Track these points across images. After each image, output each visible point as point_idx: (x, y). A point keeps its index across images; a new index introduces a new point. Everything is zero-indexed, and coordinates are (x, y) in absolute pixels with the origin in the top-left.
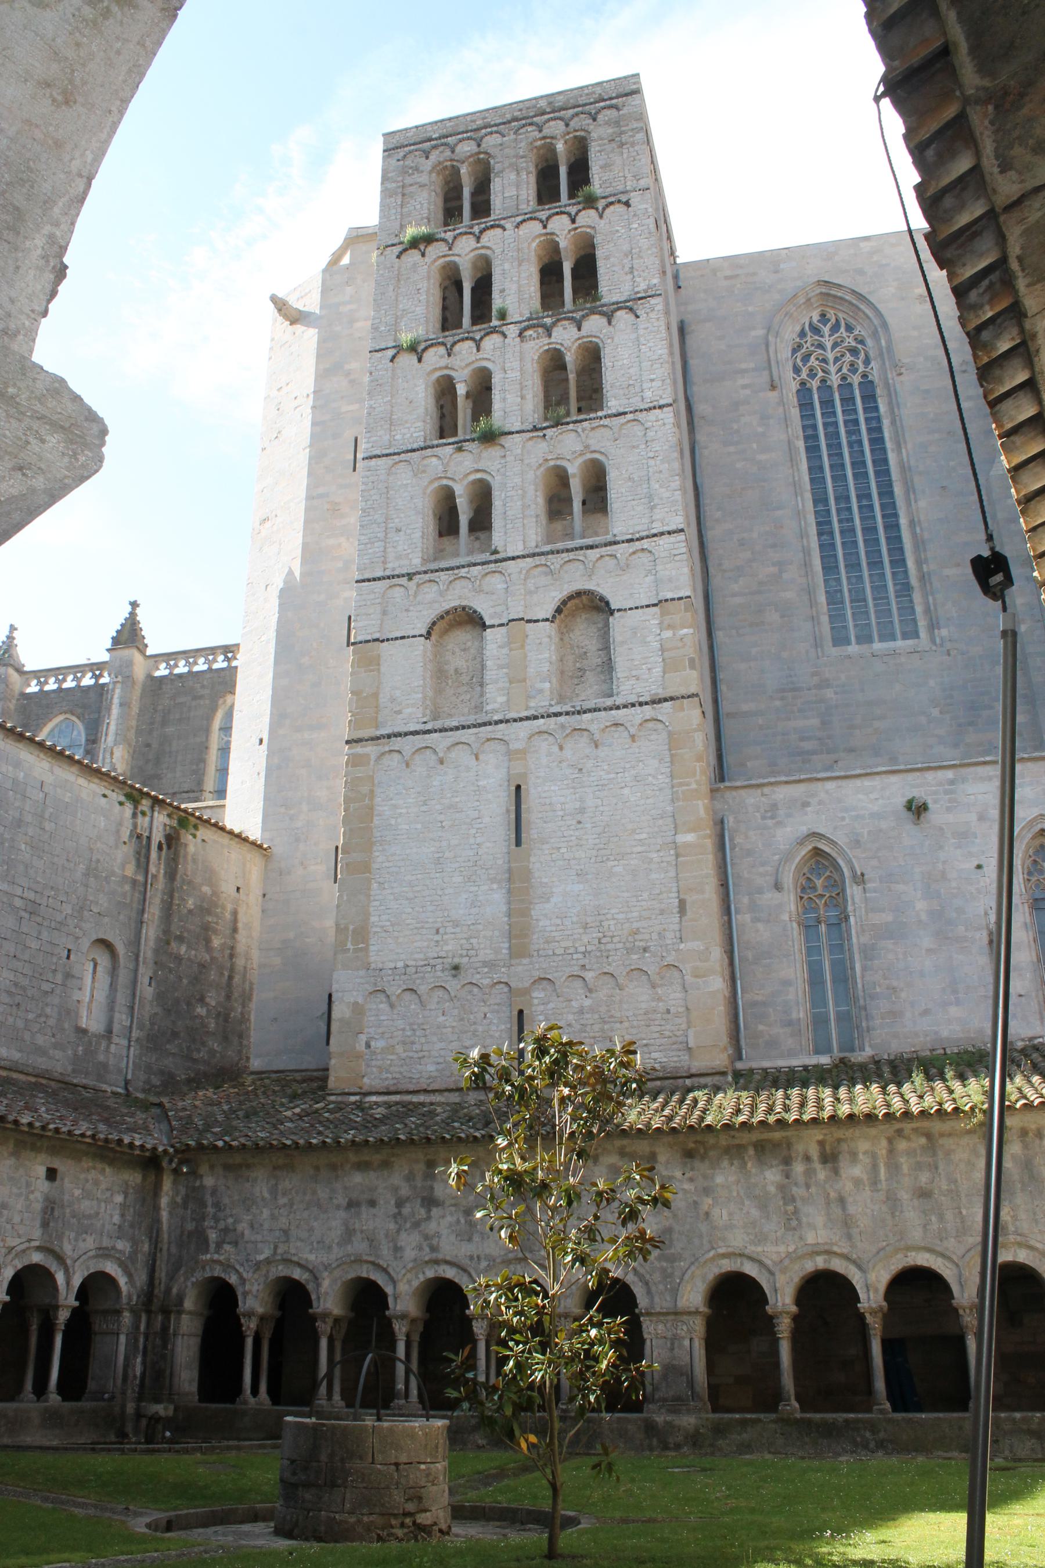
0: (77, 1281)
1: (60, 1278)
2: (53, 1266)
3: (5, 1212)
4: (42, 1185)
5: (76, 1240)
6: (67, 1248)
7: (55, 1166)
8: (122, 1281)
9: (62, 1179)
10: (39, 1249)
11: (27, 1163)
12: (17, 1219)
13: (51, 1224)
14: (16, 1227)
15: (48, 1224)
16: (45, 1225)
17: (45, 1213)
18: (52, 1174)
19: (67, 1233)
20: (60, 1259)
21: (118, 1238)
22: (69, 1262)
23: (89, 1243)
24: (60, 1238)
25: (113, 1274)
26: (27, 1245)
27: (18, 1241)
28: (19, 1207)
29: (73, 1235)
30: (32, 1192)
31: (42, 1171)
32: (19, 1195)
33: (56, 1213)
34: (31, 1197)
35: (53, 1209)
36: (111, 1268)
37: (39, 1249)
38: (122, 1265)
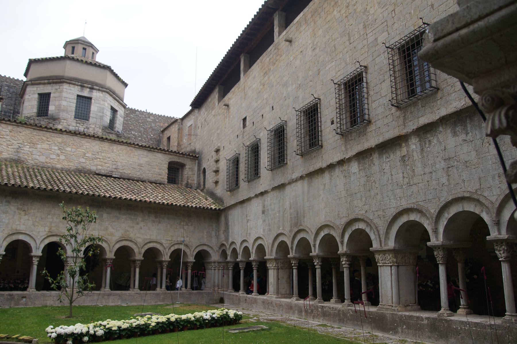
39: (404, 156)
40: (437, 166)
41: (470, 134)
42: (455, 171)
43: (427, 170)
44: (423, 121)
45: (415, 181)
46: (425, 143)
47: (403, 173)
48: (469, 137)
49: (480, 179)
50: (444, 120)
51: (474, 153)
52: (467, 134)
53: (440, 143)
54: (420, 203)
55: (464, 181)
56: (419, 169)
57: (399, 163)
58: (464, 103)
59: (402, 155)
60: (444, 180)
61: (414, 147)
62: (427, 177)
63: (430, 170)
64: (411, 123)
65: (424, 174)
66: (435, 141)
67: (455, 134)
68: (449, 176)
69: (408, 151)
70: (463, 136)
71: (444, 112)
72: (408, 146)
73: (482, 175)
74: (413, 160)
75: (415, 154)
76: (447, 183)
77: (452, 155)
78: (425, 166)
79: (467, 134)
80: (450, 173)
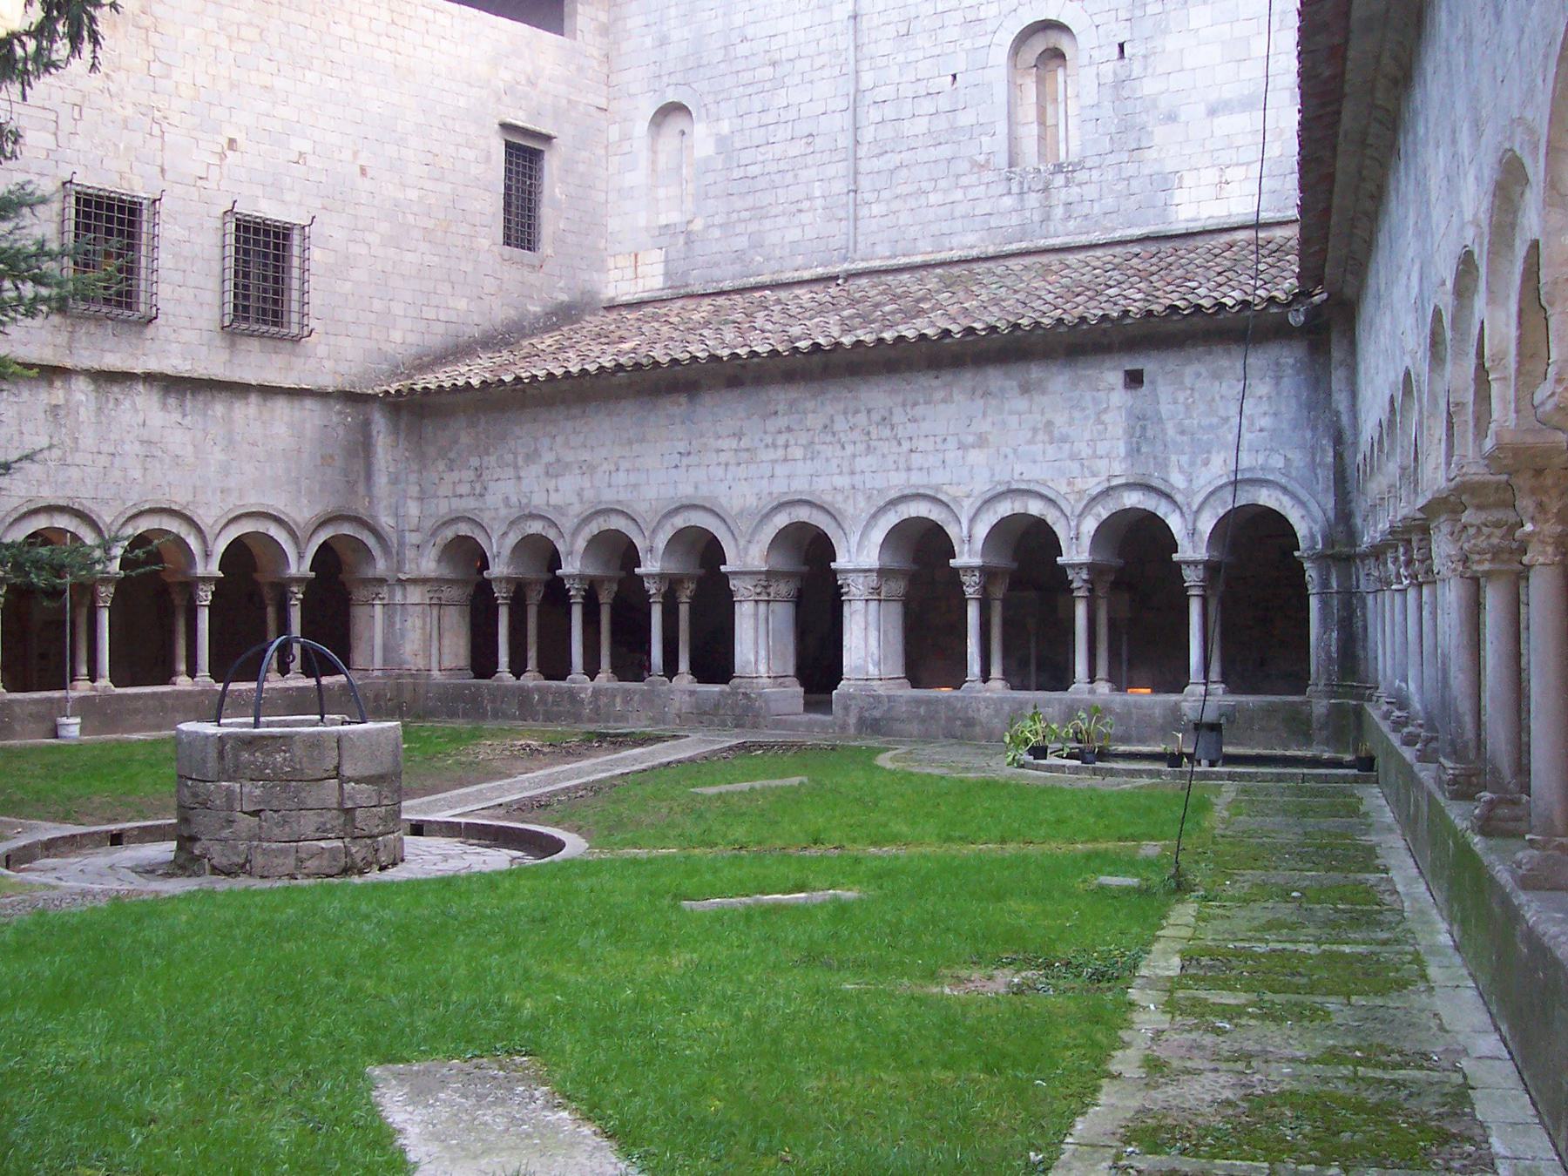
0: (1207, 524)
1: (1175, 523)
2: (1161, 509)
3: (1067, 446)
4: (1119, 397)
5: (1192, 464)
6: (1177, 480)
7: (1138, 366)
8: (1294, 516)
9: (1152, 382)
10: (1129, 486)
11: (1089, 372)
12: (1086, 451)
13: (1144, 450)
14: (1086, 463)
15: (1138, 450)
16: (1134, 451)
17: (1132, 436)
18: (1134, 379)
19: (1174, 458)
20: (1168, 497)
21: (1272, 450)
22: (1179, 498)
23: (1217, 469)
24: (1164, 465)
25: (1272, 504)
26: (1106, 485)
27: (1092, 481)
28: (1087, 436)
29: (1184, 459)
30: (1106, 410)
31: (1115, 378)
32: (1087, 418)
33: (1150, 433)
34: (1106, 418)
35: (1144, 428)
36: (1266, 498)
37: (1129, 486)
38: (1285, 490)
39: (57, 406)
40: (127, 447)
41: (189, 418)
42: (158, 465)
43: (106, 448)
44: (114, 361)
45: (77, 461)
46: (107, 401)
47: (51, 437)
48: (187, 421)
49: (195, 487)
50: (149, 378)
51: (190, 448)
52: (184, 416)
53: (136, 411)
54: (84, 501)
55: (169, 484)
56: (88, 439)
57: (42, 415)
58: (189, 367)
59: (54, 402)
60: (136, 474)
61: (83, 398)
62: (103, 460)
63: (112, 450)
64: (86, 353)
65: (99, 453)
66: (127, 404)
67: (164, 406)
68: (146, 469)
69: (67, 401)
70: (176, 416)
71: (153, 366)
72: (69, 391)
73: (198, 483)
74: (77, 419)
75: (82, 410)
76: (141, 480)
77: (155, 438)
78: (103, 439)
79: (184, 416)
80: (148, 466)
